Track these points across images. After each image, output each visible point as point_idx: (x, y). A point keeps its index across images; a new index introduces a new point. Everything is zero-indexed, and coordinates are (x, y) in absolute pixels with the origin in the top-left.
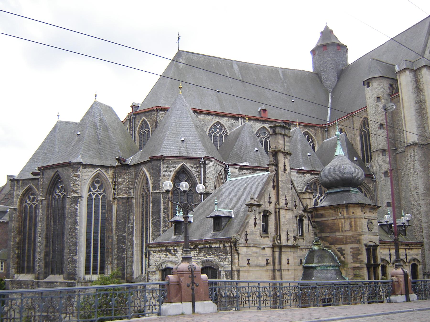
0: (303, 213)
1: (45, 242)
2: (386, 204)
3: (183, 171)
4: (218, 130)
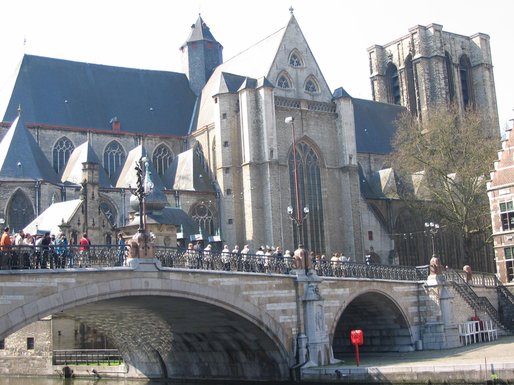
0: (111, 232)
2: (227, 221)
3: (20, 194)
4: (64, 146)
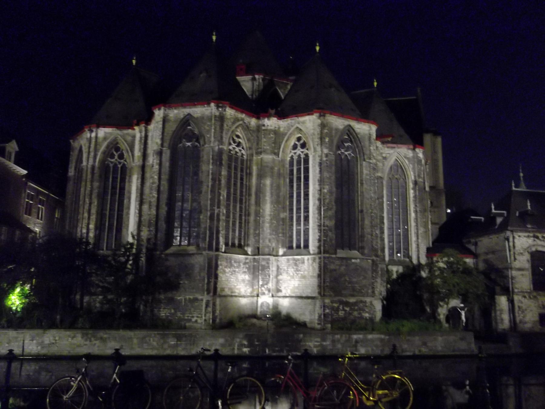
1: (334, 207)
